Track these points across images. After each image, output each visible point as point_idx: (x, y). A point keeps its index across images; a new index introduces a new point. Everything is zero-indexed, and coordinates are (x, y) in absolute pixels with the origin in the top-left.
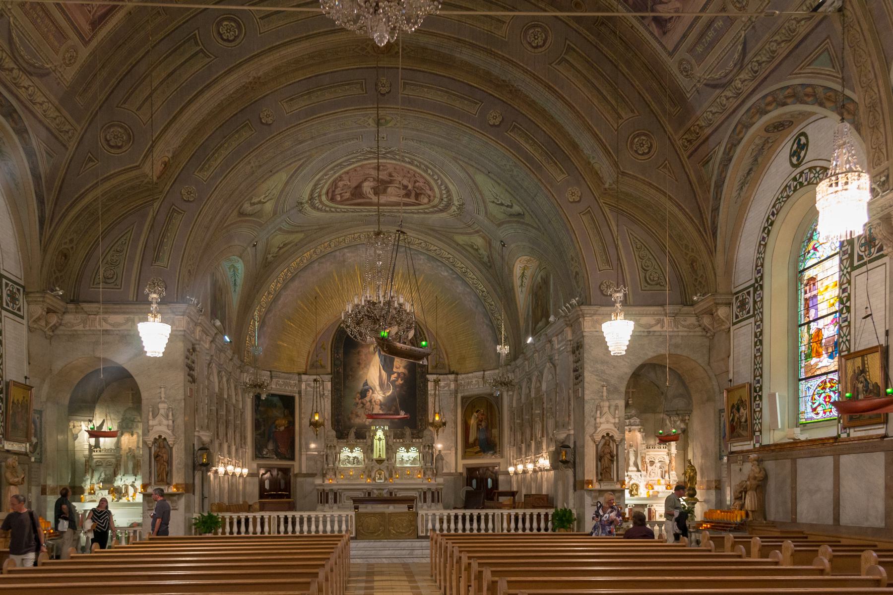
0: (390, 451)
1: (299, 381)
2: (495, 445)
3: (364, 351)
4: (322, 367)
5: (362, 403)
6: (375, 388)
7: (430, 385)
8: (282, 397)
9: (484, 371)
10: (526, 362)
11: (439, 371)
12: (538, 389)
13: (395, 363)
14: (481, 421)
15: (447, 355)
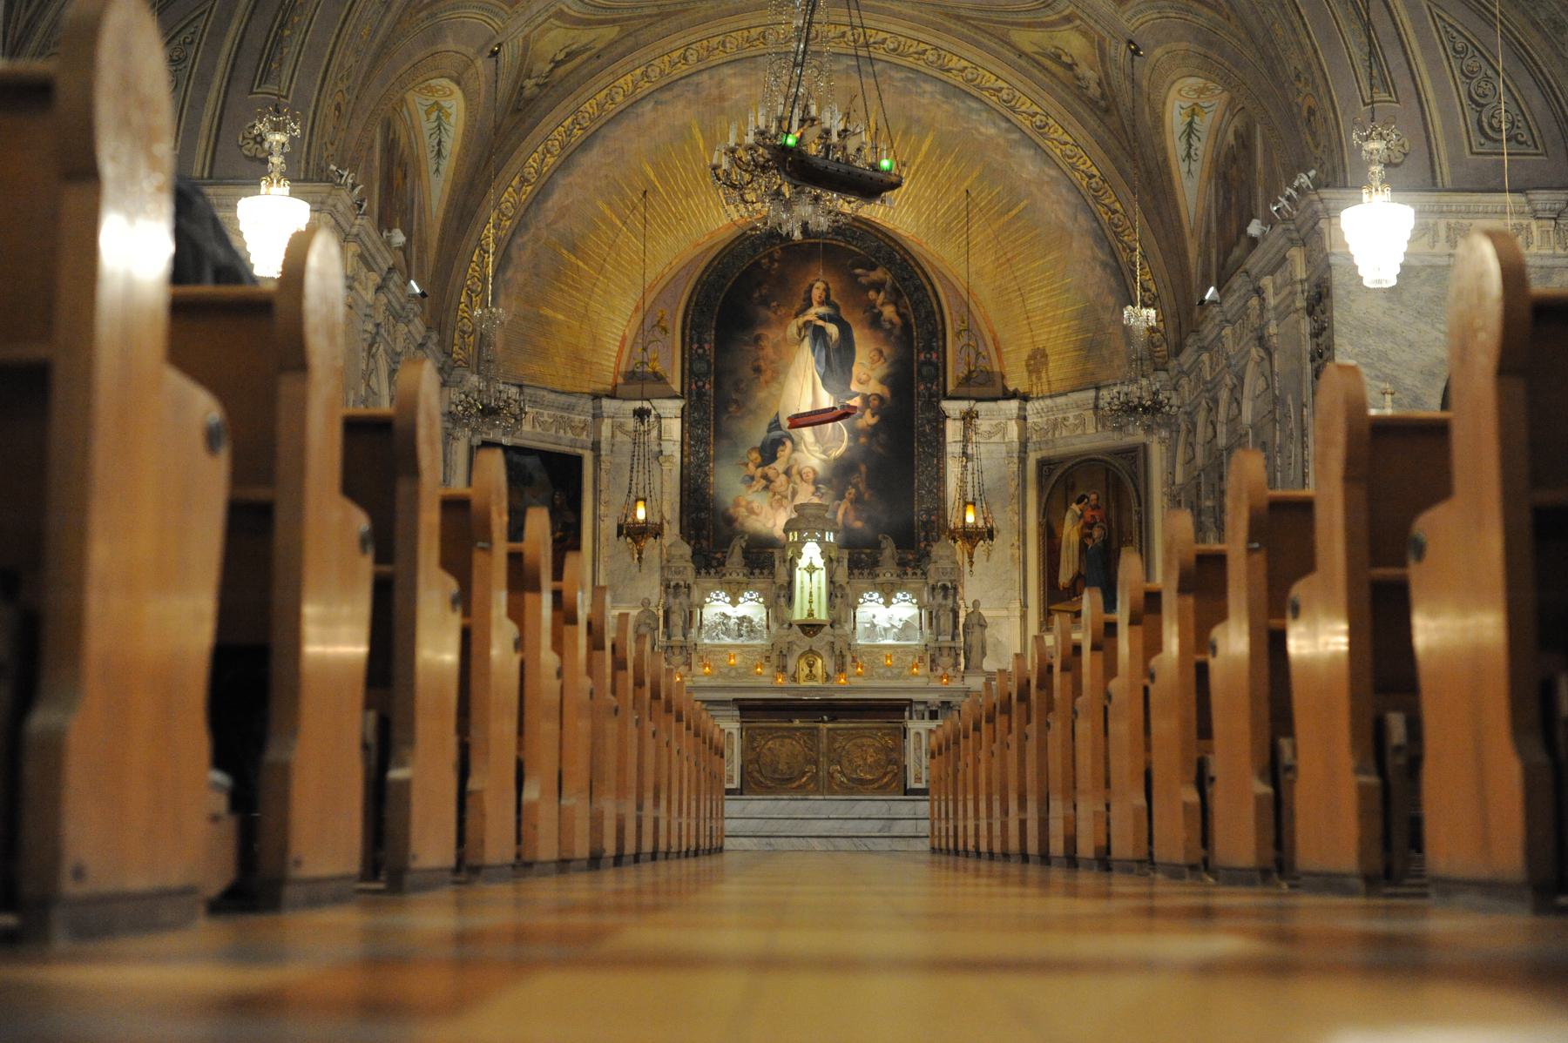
0: (838, 601)
1: (594, 416)
3: (772, 336)
4: (658, 378)
5: (765, 477)
7: (953, 430)
8: (548, 457)
9: (1098, 388)
10: (1205, 357)
11: (974, 391)
12: (1233, 421)
13: (855, 369)
14: (1090, 526)
15: (998, 349)
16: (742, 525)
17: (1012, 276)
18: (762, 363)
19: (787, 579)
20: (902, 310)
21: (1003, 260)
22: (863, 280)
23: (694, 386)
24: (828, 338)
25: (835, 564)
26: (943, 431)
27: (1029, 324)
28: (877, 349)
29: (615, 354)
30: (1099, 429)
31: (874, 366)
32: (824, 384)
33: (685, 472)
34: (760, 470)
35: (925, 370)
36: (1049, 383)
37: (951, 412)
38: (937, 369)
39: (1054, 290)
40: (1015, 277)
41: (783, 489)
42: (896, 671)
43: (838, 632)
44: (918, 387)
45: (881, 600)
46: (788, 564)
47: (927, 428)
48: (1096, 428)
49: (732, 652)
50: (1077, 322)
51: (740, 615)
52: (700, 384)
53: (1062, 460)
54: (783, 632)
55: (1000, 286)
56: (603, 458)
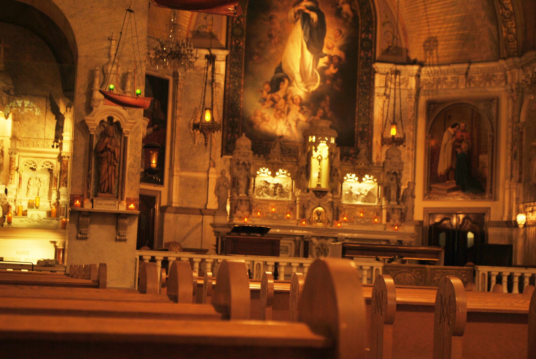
2: (484, 180)
3: (279, 16)
5: (272, 99)
6: (294, 78)
7: (379, 80)
9: (470, 63)
14: (460, 141)
16: (258, 127)
18: (273, 33)
20: (354, 8)
23: (233, 43)
24: (311, 21)
25: (333, 157)
26: (373, 80)
27: (428, 22)
29: (188, 20)
31: (336, 39)
32: (308, 48)
33: (227, 93)
34: (270, 95)
35: (365, 44)
36: (438, 57)
37: (380, 70)
38: (371, 42)
39: (447, 4)
41: (282, 107)
42: (367, 220)
43: (335, 196)
44: (360, 53)
45: (357, 179)
46: (306, 154)
47: (365, 78)
48: (466, 86)
50: (459, 24)
51: (276, 183)
52: (237, 42)
54: (303, 194)
56: (180, 82)
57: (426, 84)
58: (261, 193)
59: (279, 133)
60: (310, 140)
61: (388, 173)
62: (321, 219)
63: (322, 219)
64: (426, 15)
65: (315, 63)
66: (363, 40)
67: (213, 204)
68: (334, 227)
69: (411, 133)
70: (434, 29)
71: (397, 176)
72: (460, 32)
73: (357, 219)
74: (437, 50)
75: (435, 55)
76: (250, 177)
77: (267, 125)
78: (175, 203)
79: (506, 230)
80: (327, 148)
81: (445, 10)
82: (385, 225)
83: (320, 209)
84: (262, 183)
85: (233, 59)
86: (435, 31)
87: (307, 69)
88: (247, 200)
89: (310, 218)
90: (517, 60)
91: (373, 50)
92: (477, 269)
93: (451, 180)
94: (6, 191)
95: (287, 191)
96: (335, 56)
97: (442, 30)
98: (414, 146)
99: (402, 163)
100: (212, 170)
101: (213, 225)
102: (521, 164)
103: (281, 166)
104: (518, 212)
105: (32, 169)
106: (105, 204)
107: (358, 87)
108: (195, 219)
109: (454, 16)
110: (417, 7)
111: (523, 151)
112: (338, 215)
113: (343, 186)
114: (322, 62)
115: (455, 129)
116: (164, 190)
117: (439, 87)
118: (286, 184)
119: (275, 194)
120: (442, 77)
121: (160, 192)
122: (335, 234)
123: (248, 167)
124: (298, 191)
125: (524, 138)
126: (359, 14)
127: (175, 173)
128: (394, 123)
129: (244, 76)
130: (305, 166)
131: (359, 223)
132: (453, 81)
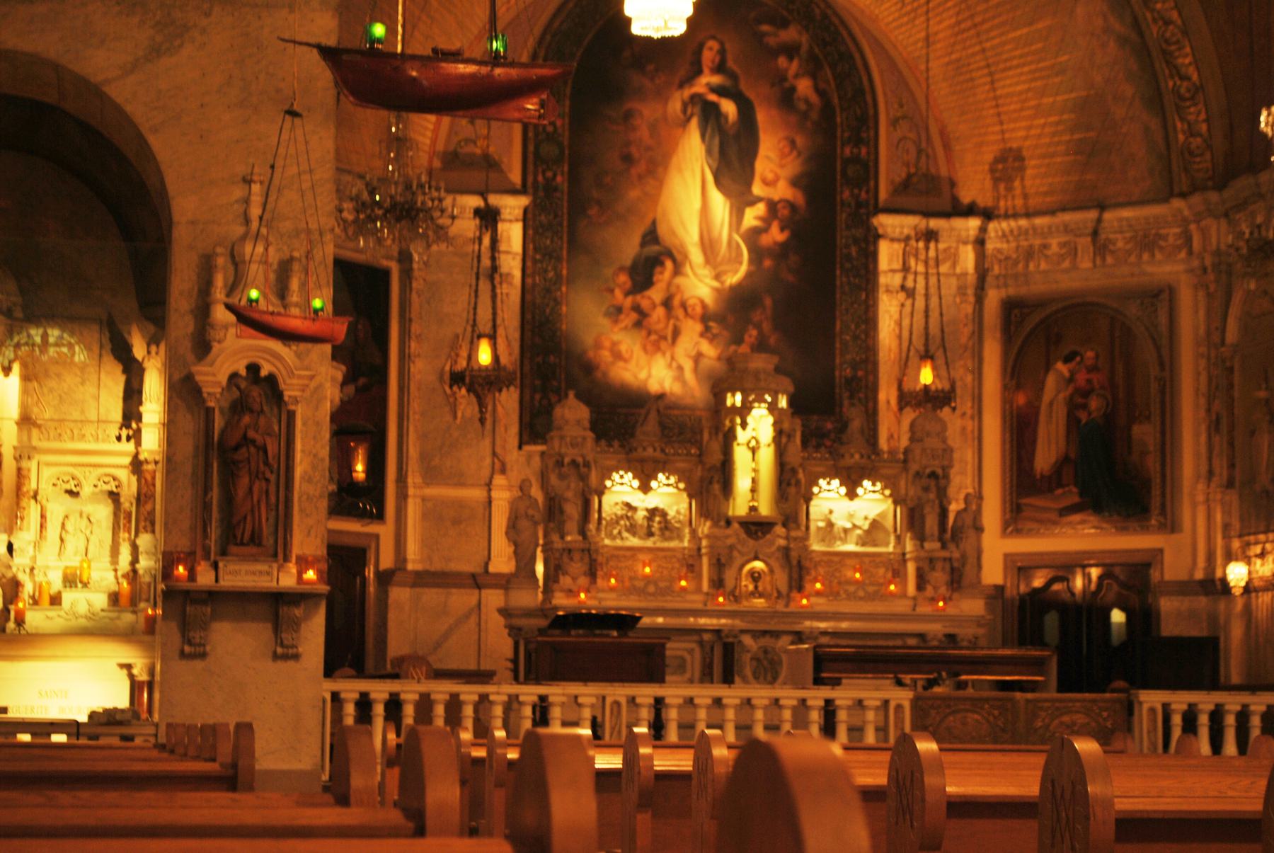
0: (792, 490)
3: (647, 111)
5: (637, 308)
6: (686, 256)
7: (887, 255)
9: (1102, 207)
14: (1086, 394)
16: (605, 374)
17: (977, 48)
18: (634, 150)
19: (721, 457)
21: (969, 23)
22: (772, 41)
23: (540, 178)
24: (723, 120)
25: (784, 440)
26: (874, 256)
27: (999, 115)
28: (787, 138)
29: (431, 127)
30: (1098, 261)
31: (784, 162)
33: (528, 297)
36: (1025, 196)
37: (889, 230)
40: (983, 51)
41: (661, 326)
42: (871, 589)
43: (793, 534)
44: (842, 193)
45: (843, 490)
46: (721, 436)
47: (854, 251)
48: (1094, 262)
49: (642, 557)
50: (1073, 116)
51: (651, 506)
53: (1039, 303)
54: (717, 531)
55: (958, 60)
56: (416, 273)
57: (1000, 261)
58: (615, 532)
59: (654, 387)
60: (729, 403)
61: (918, 475)
62: (760, 589)
63: (765, 589)
64: (995, 98)
65: (734, 219)
66: (846, 162)
67: (502, 562)
68: (792, 608)
69: (969, 378)
70: (1013, 130)
71: (937, 481)
72: (1076, 136)
73: (847, 587)
74: (1022, 179)
75: (1018, 191)
76: (590, 494)
77: (626, 369)
78: (414, 562)
79: (1202, 602)
80: (771, 420)
81: (1039, 83)
82: (914, 598)
83: (758, 565)
84: (618, 507)
85: (540, 215)
86: (1018, 135)
87: (715, 233)
88: (583, 551)
89: (735, 587)
90: (1213, 196)
91: (872, 183)
92: (1137, 697)
93: (1068, 485)
94: (10, 548)
95: (677, 525)
96: (781, 201)
97: (1033, 132)
98: (976, 407)
99: (948, 451)
100: (499, 480)
101: (505, 612)
102: (1231, 444)
103: (664, 466)
104: (1230, 557)
105: (71, 493)
106: (247, 573)
107: (838, 272)
108: (462, 599)
109: (1059, 98)
110: (972, 79)
111: (1236, 411)
112: (801, 579)
113: (812, 509)
114: (752, 217)
115: (1072, 365)
116: (385, 531)
117: (1032, 266)
118: (675, 508)
119: (650, 534)
120: (1037, 242)
121: (377, 537)
122: (795, 623)
123: (583, 470)
124: (704, 525)
125: (1237, 378)
126: (836, 101)
127: (411, 491)
128: (927, 356)
129: (569, 252)
130: (718, 465)
131: (851, 597)
132: (1063, 251)
